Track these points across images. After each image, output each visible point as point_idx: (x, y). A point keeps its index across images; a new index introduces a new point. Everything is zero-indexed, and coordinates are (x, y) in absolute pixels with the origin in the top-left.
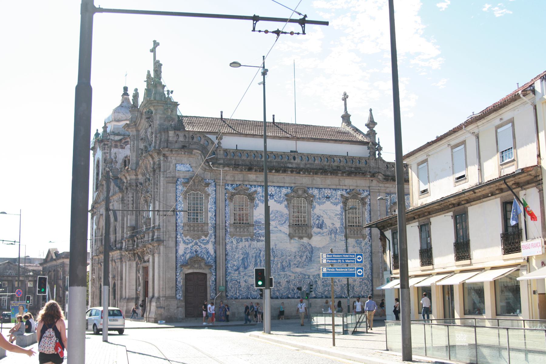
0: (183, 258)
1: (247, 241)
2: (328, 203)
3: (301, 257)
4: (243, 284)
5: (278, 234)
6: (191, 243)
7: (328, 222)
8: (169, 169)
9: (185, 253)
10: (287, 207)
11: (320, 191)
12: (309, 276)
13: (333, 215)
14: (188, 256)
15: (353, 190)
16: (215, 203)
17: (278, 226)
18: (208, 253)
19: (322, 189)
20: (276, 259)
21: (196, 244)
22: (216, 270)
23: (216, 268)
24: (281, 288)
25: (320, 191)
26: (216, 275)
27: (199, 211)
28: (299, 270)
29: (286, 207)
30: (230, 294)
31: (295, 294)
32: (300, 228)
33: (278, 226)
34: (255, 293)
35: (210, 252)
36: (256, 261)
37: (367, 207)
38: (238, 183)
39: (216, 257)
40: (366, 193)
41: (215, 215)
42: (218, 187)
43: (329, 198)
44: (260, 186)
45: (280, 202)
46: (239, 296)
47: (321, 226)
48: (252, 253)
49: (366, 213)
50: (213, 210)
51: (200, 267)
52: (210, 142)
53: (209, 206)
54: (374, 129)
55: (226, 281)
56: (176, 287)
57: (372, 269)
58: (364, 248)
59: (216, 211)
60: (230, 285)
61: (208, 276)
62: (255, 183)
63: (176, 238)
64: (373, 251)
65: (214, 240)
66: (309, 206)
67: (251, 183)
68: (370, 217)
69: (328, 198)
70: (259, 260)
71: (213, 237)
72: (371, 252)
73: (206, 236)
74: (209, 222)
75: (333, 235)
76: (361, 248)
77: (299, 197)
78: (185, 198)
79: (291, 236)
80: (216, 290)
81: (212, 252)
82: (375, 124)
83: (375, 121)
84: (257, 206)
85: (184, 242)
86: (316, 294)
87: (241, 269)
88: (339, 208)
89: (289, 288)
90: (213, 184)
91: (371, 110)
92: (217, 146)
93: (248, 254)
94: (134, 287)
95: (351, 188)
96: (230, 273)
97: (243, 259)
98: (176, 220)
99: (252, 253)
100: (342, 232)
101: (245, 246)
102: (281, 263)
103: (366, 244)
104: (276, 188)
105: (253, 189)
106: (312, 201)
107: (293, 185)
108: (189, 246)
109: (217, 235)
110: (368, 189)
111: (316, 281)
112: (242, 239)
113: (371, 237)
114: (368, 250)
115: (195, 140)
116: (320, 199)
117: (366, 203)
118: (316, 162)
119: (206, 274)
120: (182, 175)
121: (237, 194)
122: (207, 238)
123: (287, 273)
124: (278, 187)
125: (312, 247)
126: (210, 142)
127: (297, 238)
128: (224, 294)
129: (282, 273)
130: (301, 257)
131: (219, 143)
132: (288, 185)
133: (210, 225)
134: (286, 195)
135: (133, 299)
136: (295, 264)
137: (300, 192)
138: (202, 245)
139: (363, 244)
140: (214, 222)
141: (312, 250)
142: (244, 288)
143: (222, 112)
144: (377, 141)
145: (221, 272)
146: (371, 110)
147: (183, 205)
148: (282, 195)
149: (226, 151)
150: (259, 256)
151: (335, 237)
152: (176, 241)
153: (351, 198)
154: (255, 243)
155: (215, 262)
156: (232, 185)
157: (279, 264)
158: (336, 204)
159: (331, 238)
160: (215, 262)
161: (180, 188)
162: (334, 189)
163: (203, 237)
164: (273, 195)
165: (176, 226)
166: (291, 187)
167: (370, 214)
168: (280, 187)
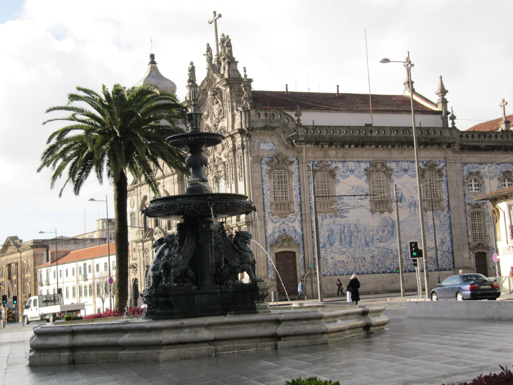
0: (272, 237)
1: (332, 217)
2: (406, 176)
3: (383, 231)
4: (330, 261)
8: (253, 148)
9: (274, 232)
10: (368, 181)
11: (397, 164)
14: (276, 235)
15: (430, 161)
16: (299, 181)
18: (295, 231)
19: (399, 161)
20: (359, 235)
22: (304, 248)
23: (303, 246)
24: (366, 263)
25: (397, 164)
26: (304, 253)
27: (284, 190)
28: (381, 245)
29: (366, 181)
31: (379, 269)
34: (342, 269)
35: (297, 230)
37: (444, 178)
38: (320, 159)
39: (303, 235)
40: (442, 165)
41: (300, 193)
42: (301, 164)
43: (407, 170)
44: (340, 162)
45: (360, 177)
46: (327, 273)
47: (400, 200)
48: (337, 229)
49: (443, 184)
50: (297, 188)
51: (289, 246)
52: (290, 119)
53: (294, 184)
54: (445, 97)
56: (268, 267)
57: (452, 241)
58: (443, 220)
59: (300, 188)
61: (297, 254)
62: (336, 159)
63: (265, 217)
64: (452, 223)
65: (300, 218)
66: (388, 180)
67: (332, 159)
68: (448, 189)
69: (405, 170)
70: (343, 237)
71: (299, 215)
72: (450, 224)
74: (294, 200)
75: (412, 208)
76: (440, 220)
77: (378, 170)
78: (271, 177)
79: (372, 211)
80: (305, 268)
81: (299, 230)
82: (447, 92)
83: (446, 89)
85: (272, 221)
87: (327, 246)
89: (373, 263)
90: (296, 162)
91: (441, 77)
92: (297, 123)
93: (332, 231)
95: (427, 159)
97: (329, 236)
98: (264, 199)
101: (330, 223)
102: (365, 238)
103: (445, 216)
104: (355, 163)
105: (334, 165)
106: (391, 175)
107: (371, 159)
108: (277, 225)
110: (443, 160)
112: (326, 216)
113: (449, 208)
114: (447, 222)
115: (276, 118)
116: (398, 172)
117: (443, 174)
118: (393, 135)
119: (294, 253)
120: (266, 154)
121: (319, 171)
122: (294, 217)
123: (370, 248)
125: (393, 222)
126: (290, 119)
127: (378, 213)
129: (366, 248)
130: (383, 231)
131: (299, 120)
132: (366, 159)
133: (295, 203)
134: (366, 170)
136: (378, 239)
137: (379, 166)
138: (289, 223)
139: (442, 216)
140: (299, 200)
142: (331, 265)
143: (287, 85)
144: (449, 110)
147: (268, 185)
148: (362, 170)
149: (306, 127)
150: (344, 232)
151: (415, 210)
153: (428, 170)
154: (339, 219)
155: (303, 240)
157: (363, 239)
159: (410, 211)
160: (303, 240)
161: (265, 167)
162: (410, 162)
164: (353, 171)
165: (264, 205)
166: (370, 162)
167: (447, 185)
168: (359, 162)
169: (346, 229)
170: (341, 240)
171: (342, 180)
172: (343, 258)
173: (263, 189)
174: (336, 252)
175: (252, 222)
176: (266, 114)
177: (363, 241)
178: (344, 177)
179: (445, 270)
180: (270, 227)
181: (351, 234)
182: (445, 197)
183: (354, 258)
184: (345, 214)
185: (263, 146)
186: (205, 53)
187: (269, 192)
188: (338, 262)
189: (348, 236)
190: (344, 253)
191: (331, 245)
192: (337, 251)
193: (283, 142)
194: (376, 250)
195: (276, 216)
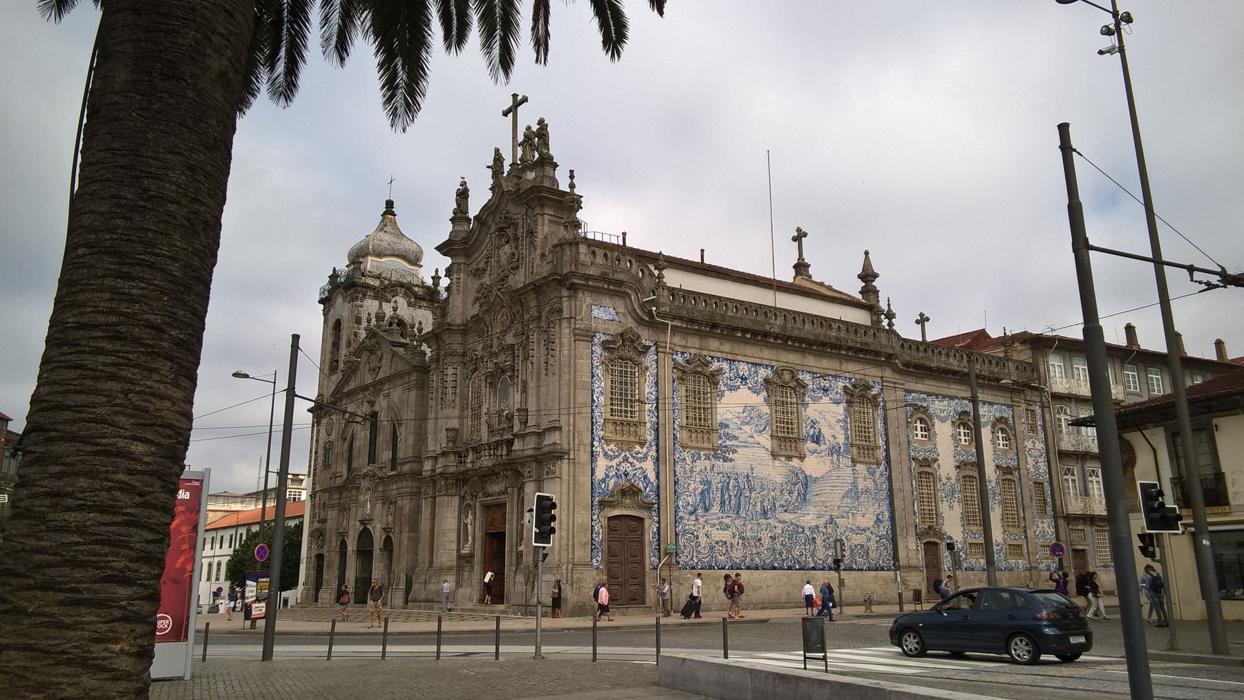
3: (790, 493)
5: (755, 450)
6: (616, 457)
7: (827, 433)
9: (607, 476)
12: (803, 528)
13: (833, 421)
16: (657, 384)
17: (755, 435)
18: (645, 477)
21: (626, 459)
26: (659, 522)
28: (788, 517)
30: (683, 559)
32: (788, 441)
33: (755, 435)
36: (723, 495)
37: (880, 411)
41: (657, 408)
45: (758, 393)
47: (817, 439)
48: (716, 481)
52: (647, 273)
53: (647, 390)
55: (677, 534)
57: (892, 518)
59: (657, 398)
60: (682, 541)
61: (647, 523)
62: (719, 355)
65: (655, 454)
67: (713, 354)
73: (642, 444)
74: (647, 419)
77: (783, 388)
79: (774, 456)
81: (652, 476)
82: (876, 276)
84: (722, 395)
85: (606, 455)
86: (815, 562)
88: (841, 409)
90: (653, 349)
91: (867, 253)
93: (709, 483)
94: (454, 546)
96: (681, 518)
98: (593, 411)
99: (716, 481)
100: (847, 452)
103: (881, 474)
105: (715, 365)
108: (614, 463)
109: (661, 444)
111: (814, 538)
115: (622, 265)
118: (807, 327)
119: (641, 520)
120: (601, 327)
122: (645, 450)
124: (753, 364)
126: (647, 273)
128: (674, 561)
129: (763, 521)
130: (790, 493)
132: (767, 362)
133: (648, 425)
135: (450, 568)
137: (787, 376)
139: (877, 475)
141: (806, 482)
145: (667, 517)
146: (867, 253)
152: (592, 452)
153: (857, 396)
154: (721, 462)
155: (658, 495)
156: (683, 353)
158: (837, 403)
160: (658, 495)
163: (638, 448)
169: (732, 482)
170: (723, 503)
171: (727, 393)
172: (725, 535)
173: (593, 391)
174: (714, 525)
175: (568, 453)
176: (605, 255)
177: (758, 508)
178: (733, 388)
179: (882, 569)
180: (602, 464)
181: (740, 494)
182: (881, 442)
183: (743, 538)
184: (731, 456)
185: (596, 312)
186: (491, 163)
187: (602, 398)
188: (717, 543)
189: (735, 495)
190: (727, 527)
191: (707, 510)
192: (716, 521)
193: (634, 310)
194: (780, 526)
195: (612, 446)
